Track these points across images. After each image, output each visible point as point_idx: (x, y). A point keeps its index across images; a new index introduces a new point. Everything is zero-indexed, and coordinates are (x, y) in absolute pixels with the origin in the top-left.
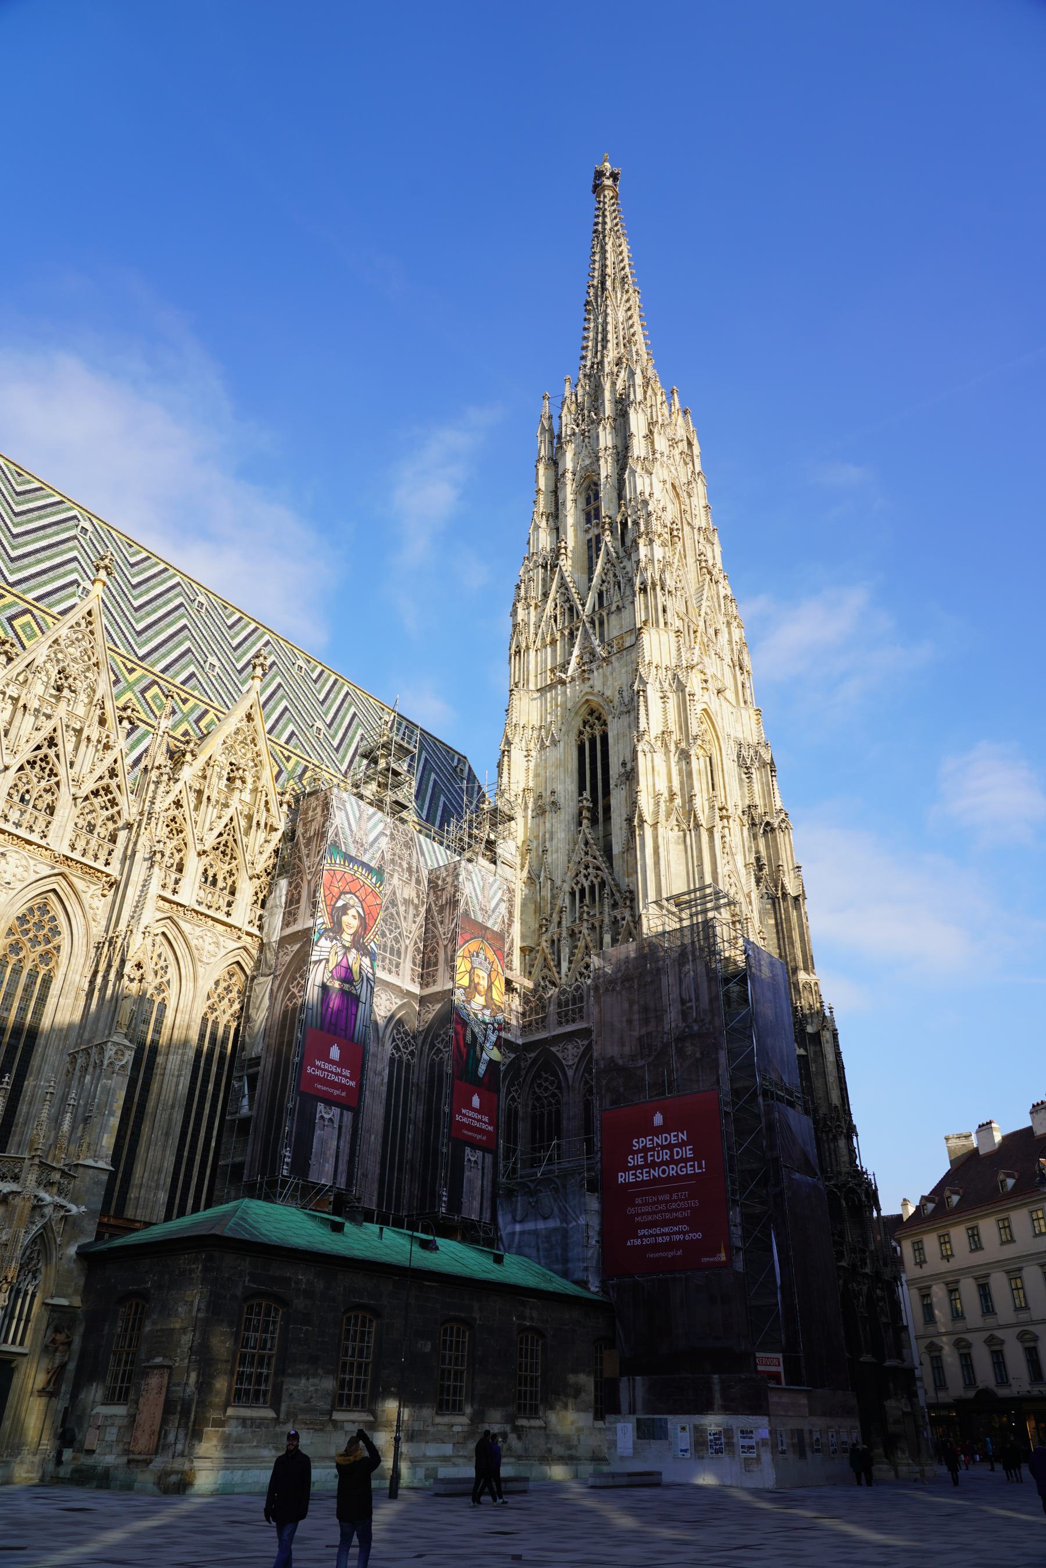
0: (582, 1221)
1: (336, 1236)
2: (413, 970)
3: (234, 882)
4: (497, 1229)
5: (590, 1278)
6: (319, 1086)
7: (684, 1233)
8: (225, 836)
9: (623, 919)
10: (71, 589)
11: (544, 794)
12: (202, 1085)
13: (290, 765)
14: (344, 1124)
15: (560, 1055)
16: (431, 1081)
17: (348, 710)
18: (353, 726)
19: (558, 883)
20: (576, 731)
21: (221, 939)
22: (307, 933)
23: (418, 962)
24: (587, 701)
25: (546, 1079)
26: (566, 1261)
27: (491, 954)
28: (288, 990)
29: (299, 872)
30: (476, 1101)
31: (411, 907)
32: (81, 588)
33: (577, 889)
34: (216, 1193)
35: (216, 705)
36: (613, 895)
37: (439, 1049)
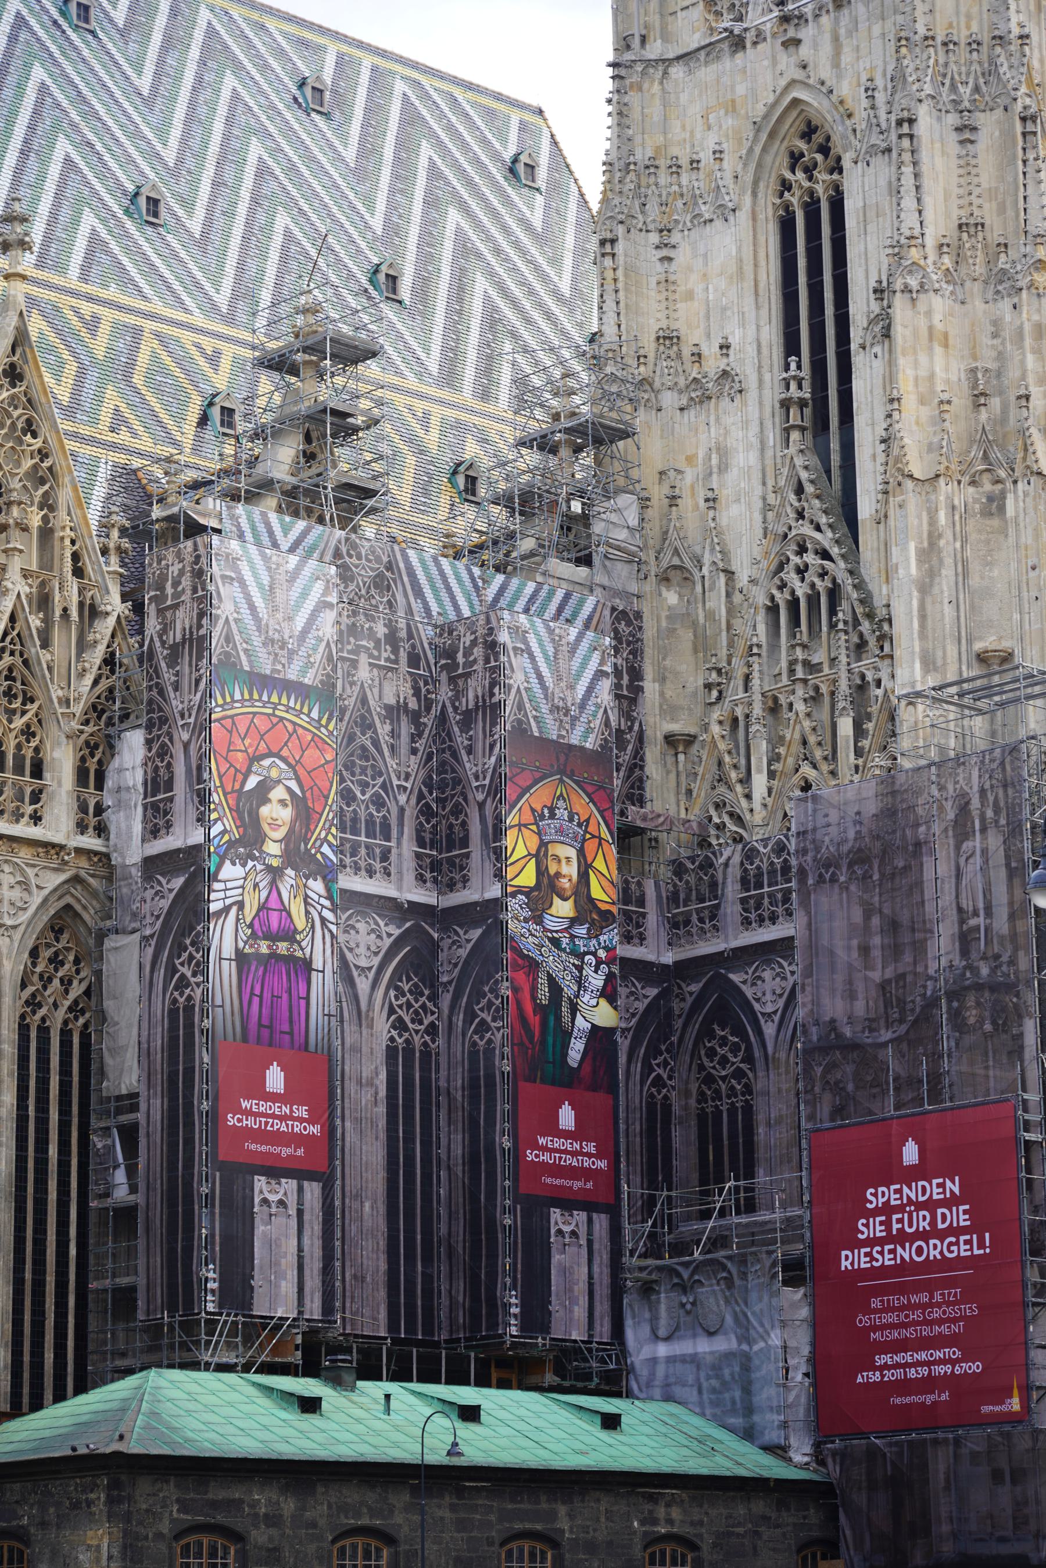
0: (775, 1339)
1: (312, 1419)
2: (418, 856)
3: (37, 750)
4: (624, 1352)
5: (793, 1441)
6: (253, 1147)
7: (953, 1362)
9: (878, 684)
11: (705, 350)
12: (36, 1151)
13: (100, 345)
14: (307, 1206)
15: (748, 992)
16: (473, 1086)
17: (217, 92)
18: (235, 144)
19: (743, 578)
20: (774, 185)
21: (30, 872)
22: (193, 854)
23: (427, 836)
24: (796, 102)
25: (724, 1041)
26: (749, 1410)
27: (583, 806)
28: (172, 970)
29: (164, 720)
30: (567, 1117)
31: (404, 721)
33: (781, 598)
34: (91, 1336)
36: (856, 623)
37: (483, 1022)
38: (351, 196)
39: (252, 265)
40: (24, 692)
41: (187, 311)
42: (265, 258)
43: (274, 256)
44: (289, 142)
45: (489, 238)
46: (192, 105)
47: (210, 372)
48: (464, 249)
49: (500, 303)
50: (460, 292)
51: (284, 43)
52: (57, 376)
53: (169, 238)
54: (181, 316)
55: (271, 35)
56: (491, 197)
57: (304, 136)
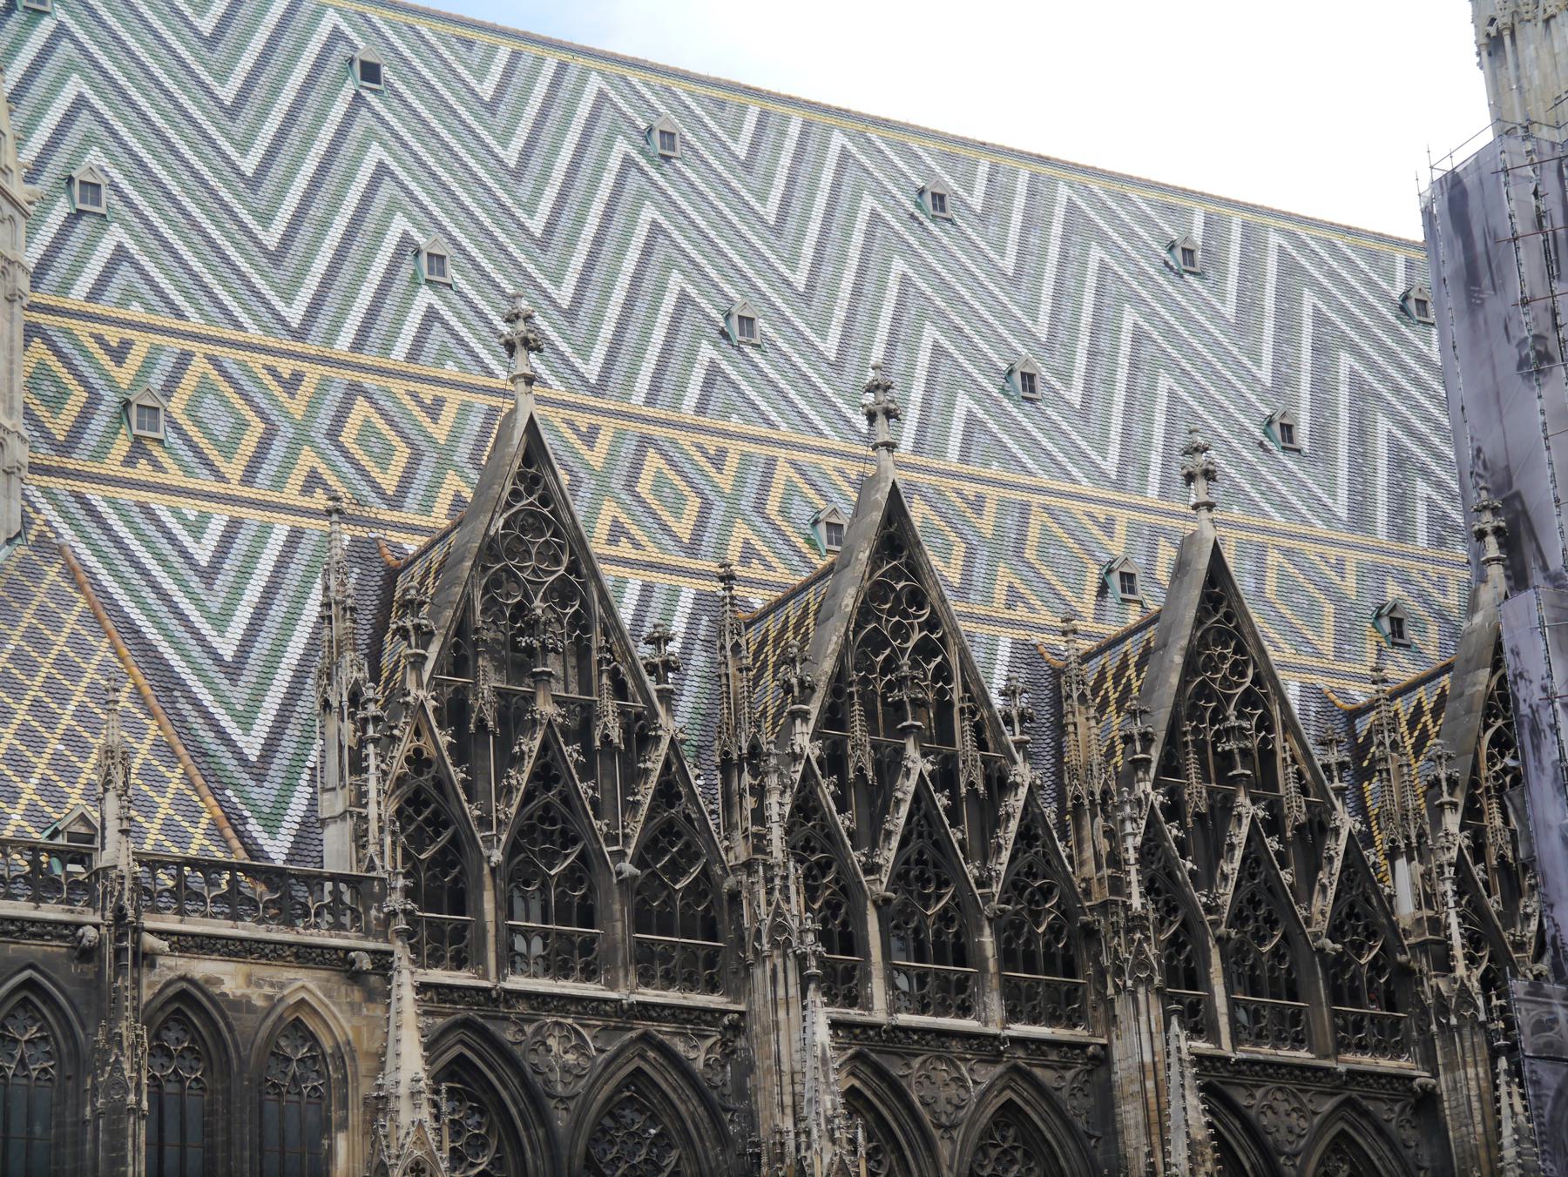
8: (915, 844)
10: (406, 271)
13: (987, 524)
17: (1084, 265)
32: (424, 258)
35: (784, 432)
38: (1235, 351)
39: (1138, 430)
40: (938, 876)
41: (1074, 481)
42: (1150, 420)
43: (1160, 419)
44: (1164, 305)
45: (1385, 378)
46: (1059, 282)
47: (1105, 539)
48: (1360, 390)
49: (1406, 441)
50: (1361, 433)
51: (1148, 210)
52: (946, 559)
53: (1049, 411)
54: (1067, 487)
55: (1134, 203)
56: (1384, 337)
57: (1179, 298)
